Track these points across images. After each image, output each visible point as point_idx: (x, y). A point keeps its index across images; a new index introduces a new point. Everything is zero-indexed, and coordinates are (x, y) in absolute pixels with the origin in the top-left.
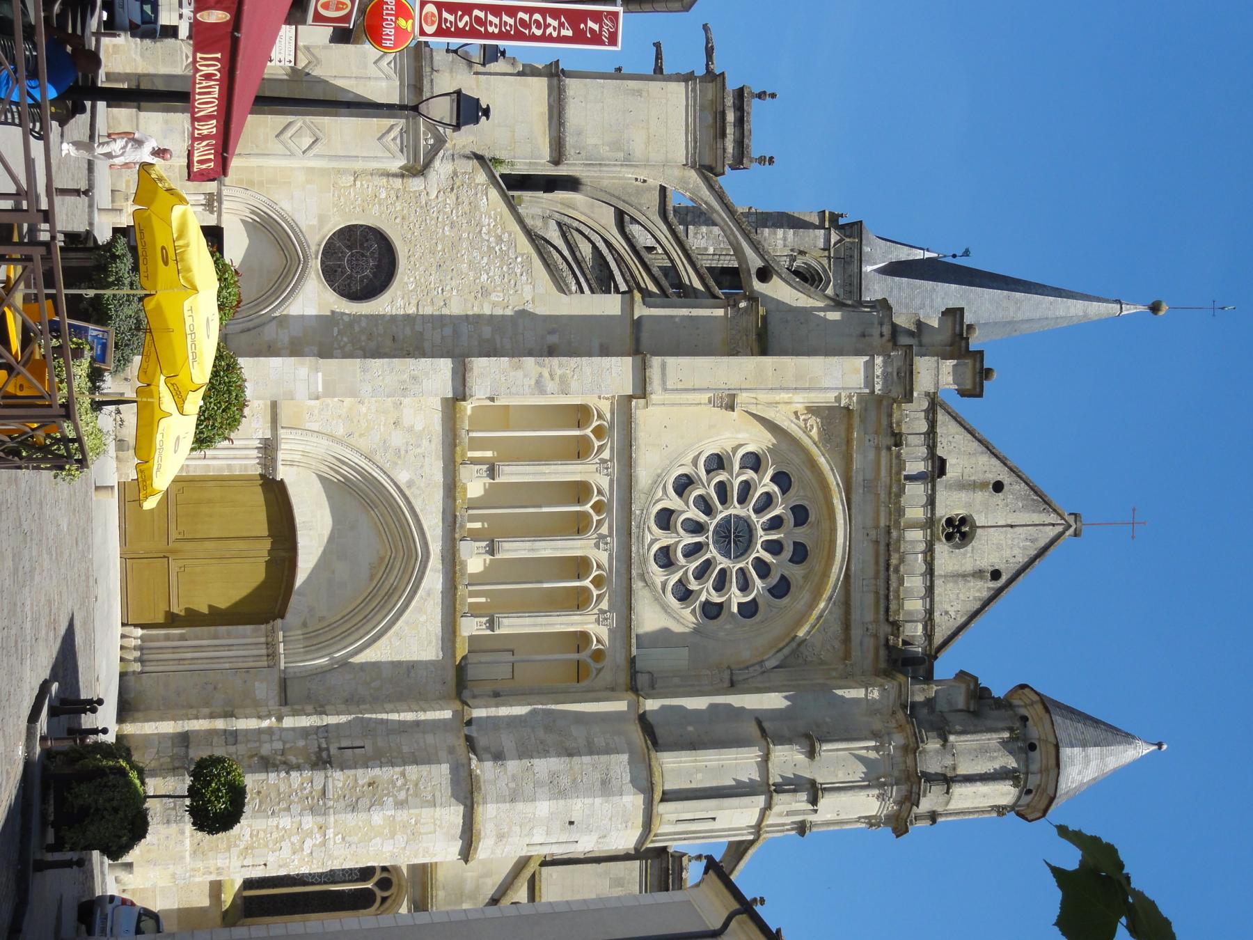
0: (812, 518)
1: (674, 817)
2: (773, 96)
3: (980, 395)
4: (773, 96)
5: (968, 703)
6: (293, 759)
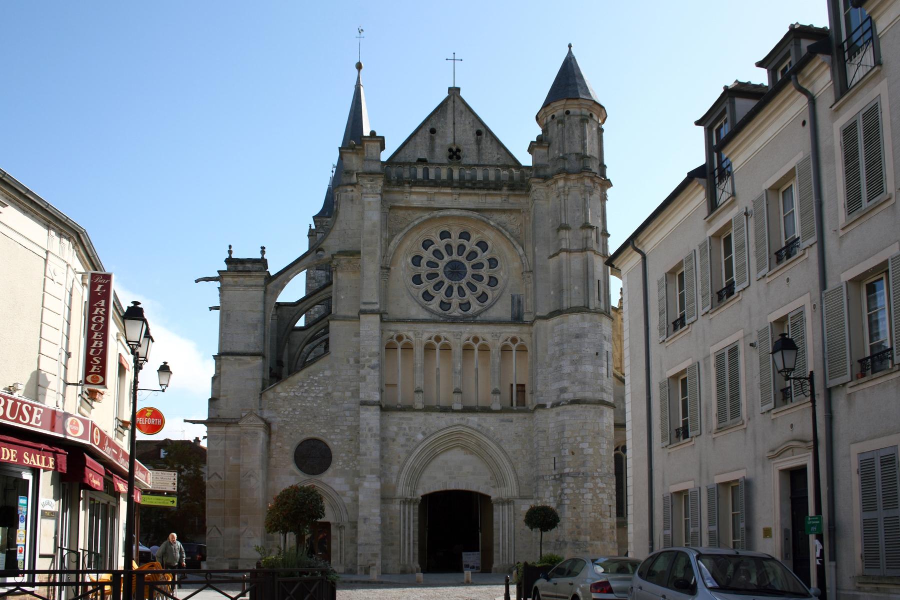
0: (447, 229)
1: (597, 301)
2: (230, 247)
3: (383, 138)
4: (230, 247)
5: (544, 147)
6: (560, 491)
